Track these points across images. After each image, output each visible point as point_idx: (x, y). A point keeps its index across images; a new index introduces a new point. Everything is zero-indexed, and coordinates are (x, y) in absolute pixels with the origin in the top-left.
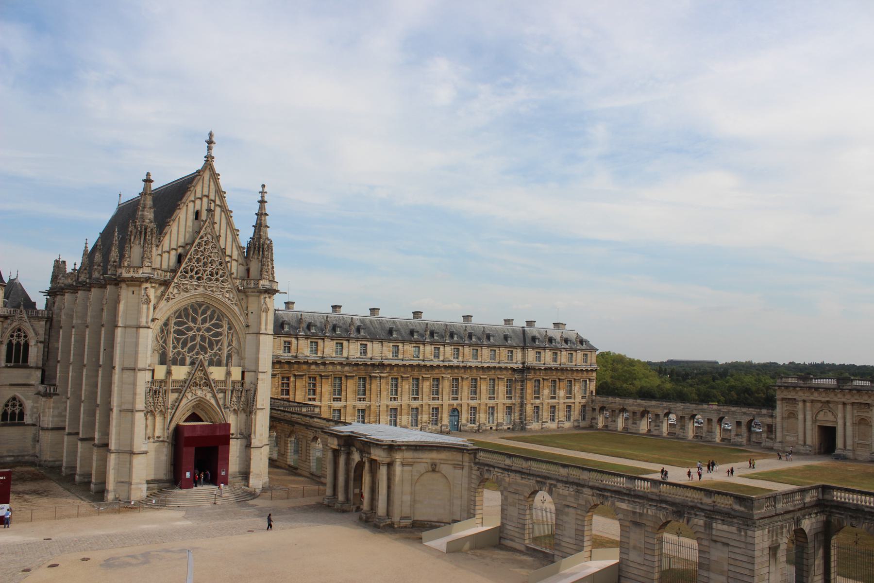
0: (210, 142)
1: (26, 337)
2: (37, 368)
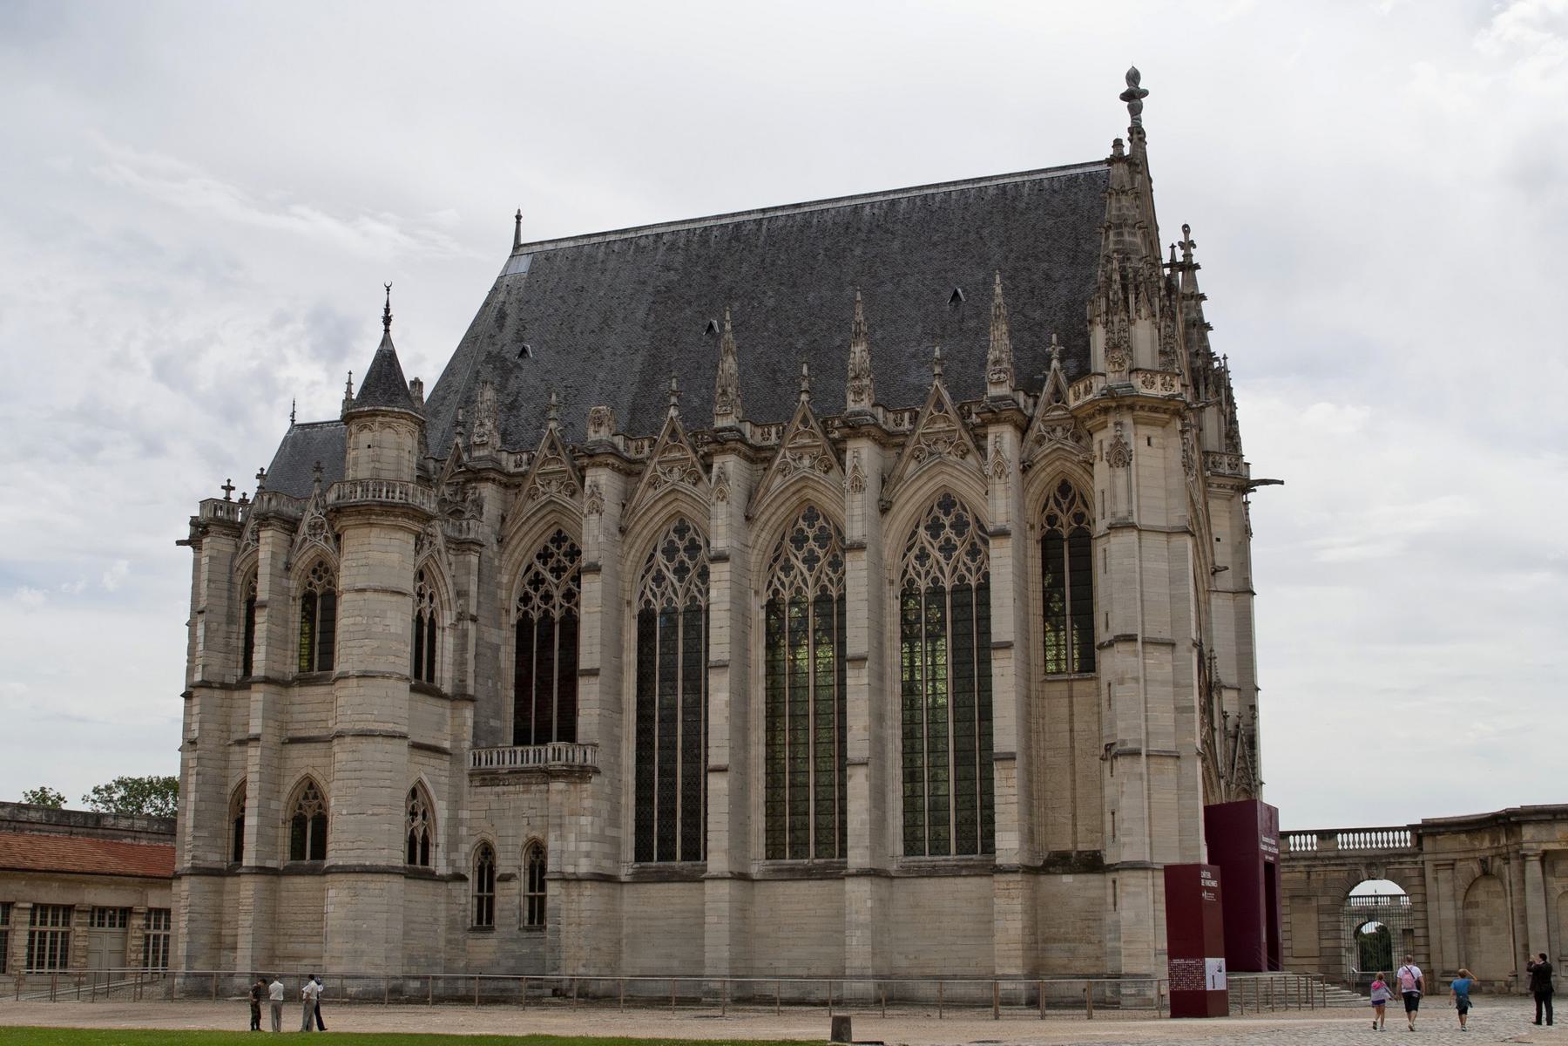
0: (1134, 97)
1: (431, 598)
2: (461, 696)
